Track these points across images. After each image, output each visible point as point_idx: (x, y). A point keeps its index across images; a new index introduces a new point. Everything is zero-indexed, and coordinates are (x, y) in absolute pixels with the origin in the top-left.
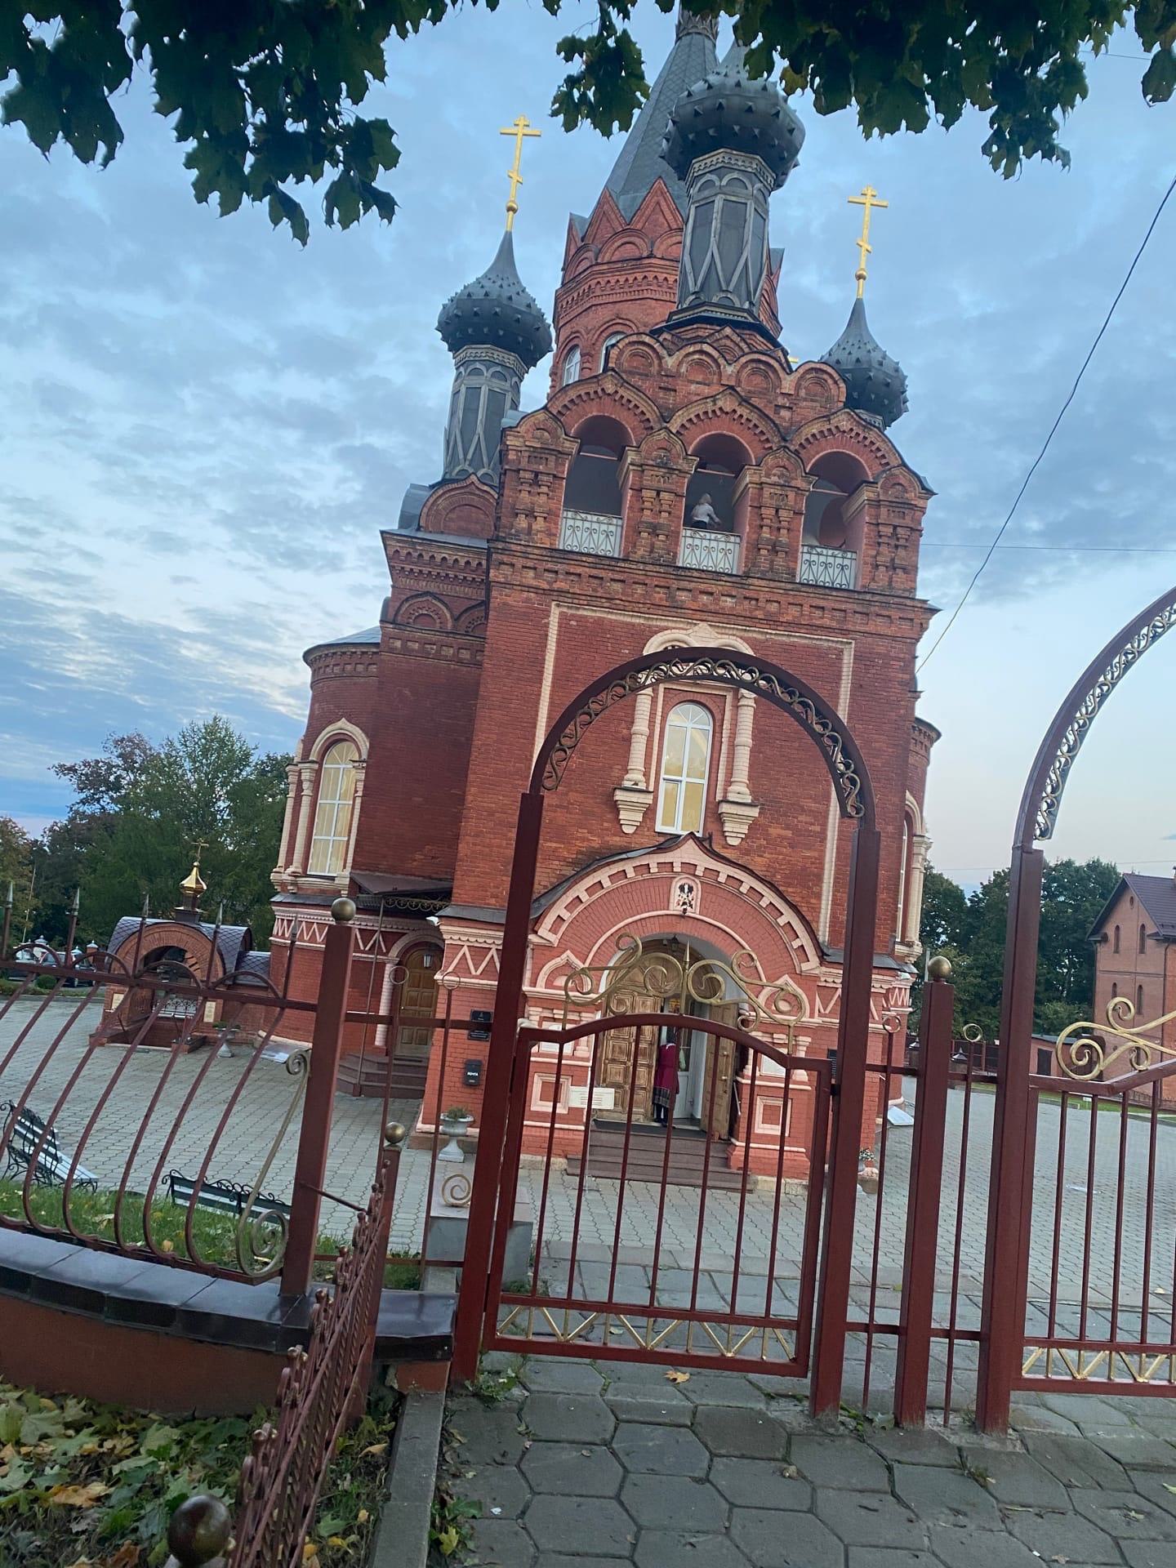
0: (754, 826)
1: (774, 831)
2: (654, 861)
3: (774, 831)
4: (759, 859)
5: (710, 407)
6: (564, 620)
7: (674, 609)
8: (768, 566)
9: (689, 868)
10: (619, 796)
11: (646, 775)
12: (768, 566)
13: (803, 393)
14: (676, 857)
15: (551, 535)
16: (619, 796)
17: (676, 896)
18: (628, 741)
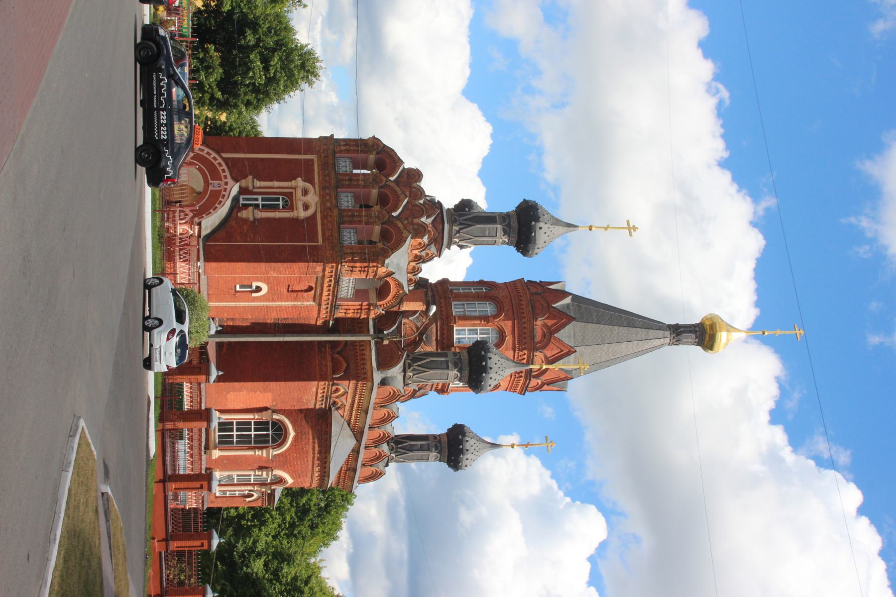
0: (245, 221)
1: (245, 227)
2: (227, 173)
3: (245, 227)
4: (234, 223)
5: (400, 193)
6: (312, 160)
7: (323, 188)
8: (346, 218)
9: (226, 183)
10: (250, 177)
11: (260, 188)
12: (346, 218)
13: (416, 227)
14: (229, 180)
15: (341, 152)
16: (250, 177)
17: (216, 182)
18: (271, 180)
